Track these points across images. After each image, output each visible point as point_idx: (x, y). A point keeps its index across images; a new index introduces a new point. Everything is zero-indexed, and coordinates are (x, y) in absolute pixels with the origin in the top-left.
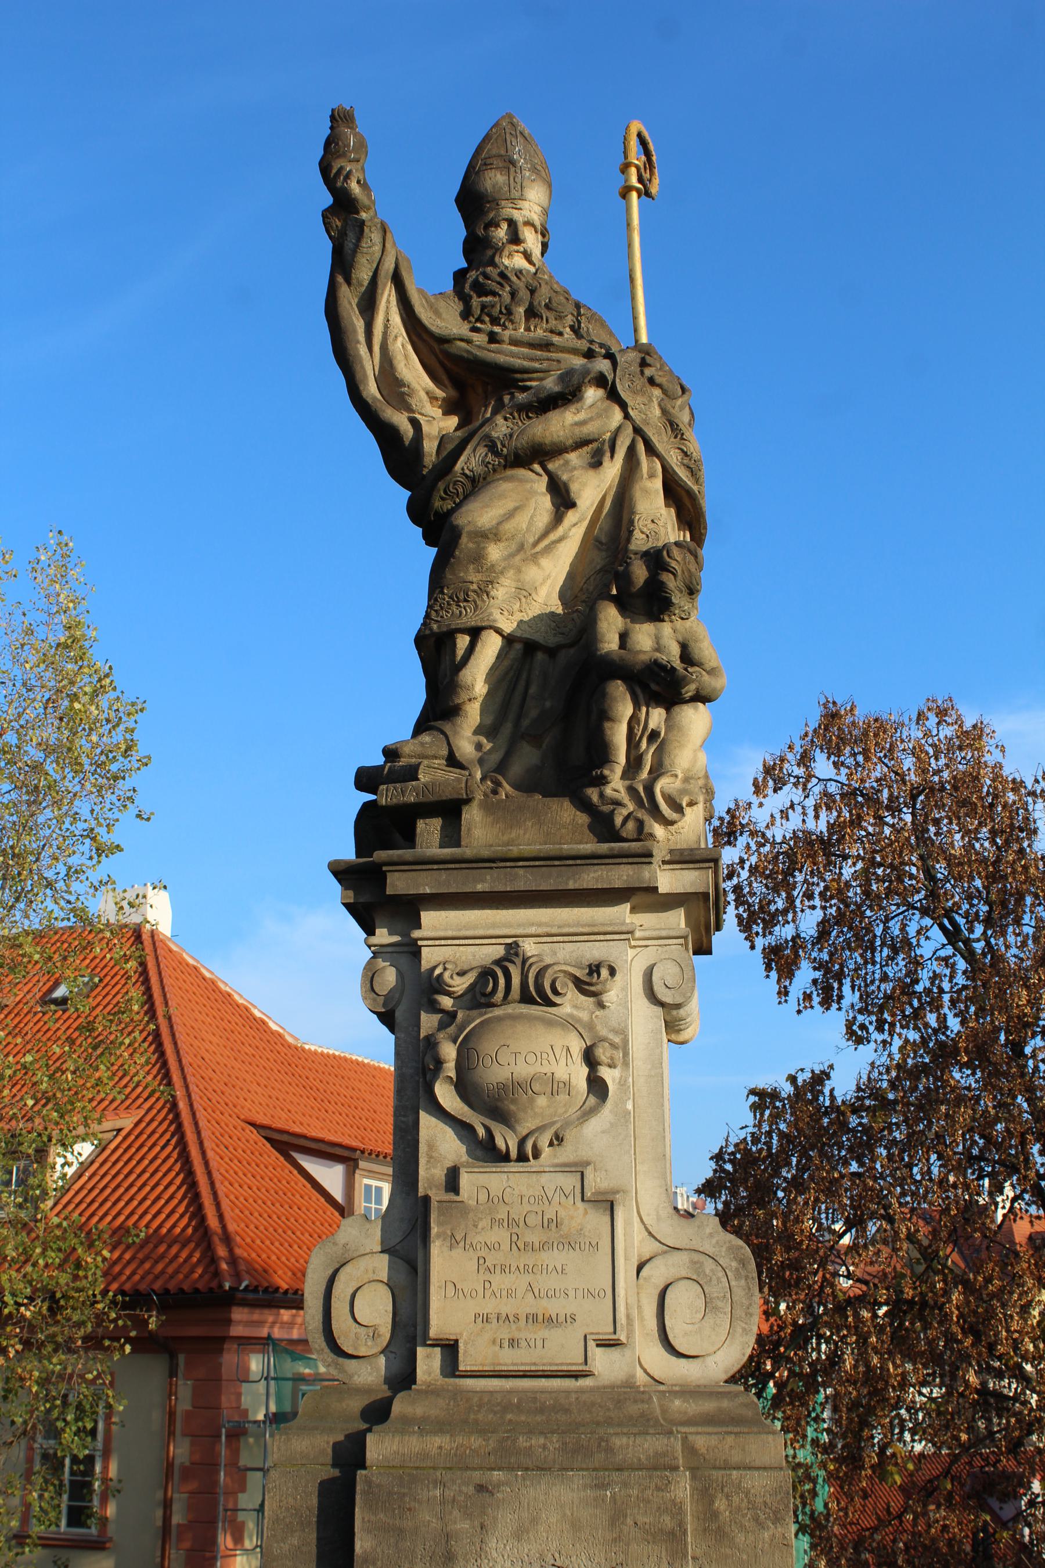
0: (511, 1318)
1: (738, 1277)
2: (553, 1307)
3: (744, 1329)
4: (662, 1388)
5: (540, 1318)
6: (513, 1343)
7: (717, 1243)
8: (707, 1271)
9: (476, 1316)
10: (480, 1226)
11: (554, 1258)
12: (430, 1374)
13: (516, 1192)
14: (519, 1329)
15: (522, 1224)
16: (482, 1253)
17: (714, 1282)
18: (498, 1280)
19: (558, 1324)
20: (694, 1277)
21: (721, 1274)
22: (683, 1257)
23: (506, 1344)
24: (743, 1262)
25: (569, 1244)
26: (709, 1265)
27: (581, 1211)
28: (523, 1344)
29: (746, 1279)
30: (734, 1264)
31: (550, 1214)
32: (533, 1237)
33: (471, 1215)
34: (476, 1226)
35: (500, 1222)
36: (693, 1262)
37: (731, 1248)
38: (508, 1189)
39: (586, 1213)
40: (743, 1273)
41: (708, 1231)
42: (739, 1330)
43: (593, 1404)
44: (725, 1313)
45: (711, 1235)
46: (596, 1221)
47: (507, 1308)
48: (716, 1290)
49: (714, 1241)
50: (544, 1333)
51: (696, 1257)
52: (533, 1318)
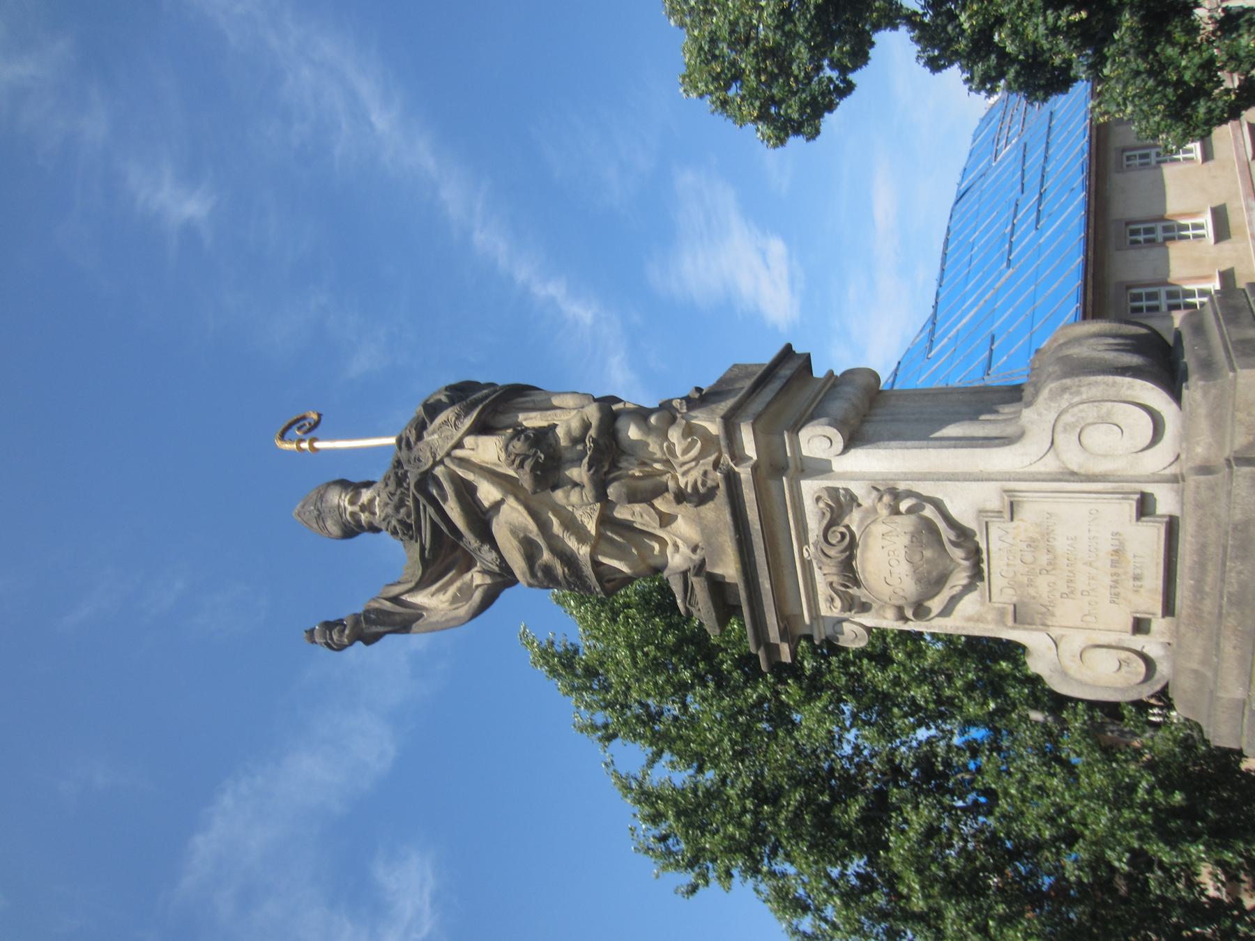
0: (1115, 578)
1: (1078, 393)
2: (1107, 546)
3: (1129, 388)
4: (1183, 457)
5: (1114, 558)
6: (1137, 578)
7: (1046, 410)
8: (1073, 420)
9: (1112, 602)
10: (1035, 594)
11: (1061, 544)
12: (1163, 633)
13: (1005, 568)
14: (1126, 573)
15: (1032, 566)
16: (1058, 595)
17: (1083, 414)
18: (1081, 583)
19: (1122, 544)
20: (1078, 430)
21: (1076, 410)
22: (1059, 438)
23: (1138, 583)
24: (1064, 389)
25: (1047, 535)
26: (1067, 418)
27: (1020, 523)
28: (1138, 571)
29: (1079, 386)
30: (1066, 396)
31: (1024, 546)
32: (1044, 559)
33: (1025, 600)
34: (1034, 598)
35: (1030, 580)
36: (1065, 430)
37: (1053, 396)
38: (1003, 574)
39: (1022, 520)
40: (1074, 389)
41: (1036, 417)
42: (1129, 392)
43: (1199, 525)
44: (1113, 407)
45: (1040, 414)
46: (1028, 513)
47: (1107, 581)
48: (1090, 412)
49: (1045, 412)
50: (1129, 555)
51: (1059, 428)
52: (1114, 564)
